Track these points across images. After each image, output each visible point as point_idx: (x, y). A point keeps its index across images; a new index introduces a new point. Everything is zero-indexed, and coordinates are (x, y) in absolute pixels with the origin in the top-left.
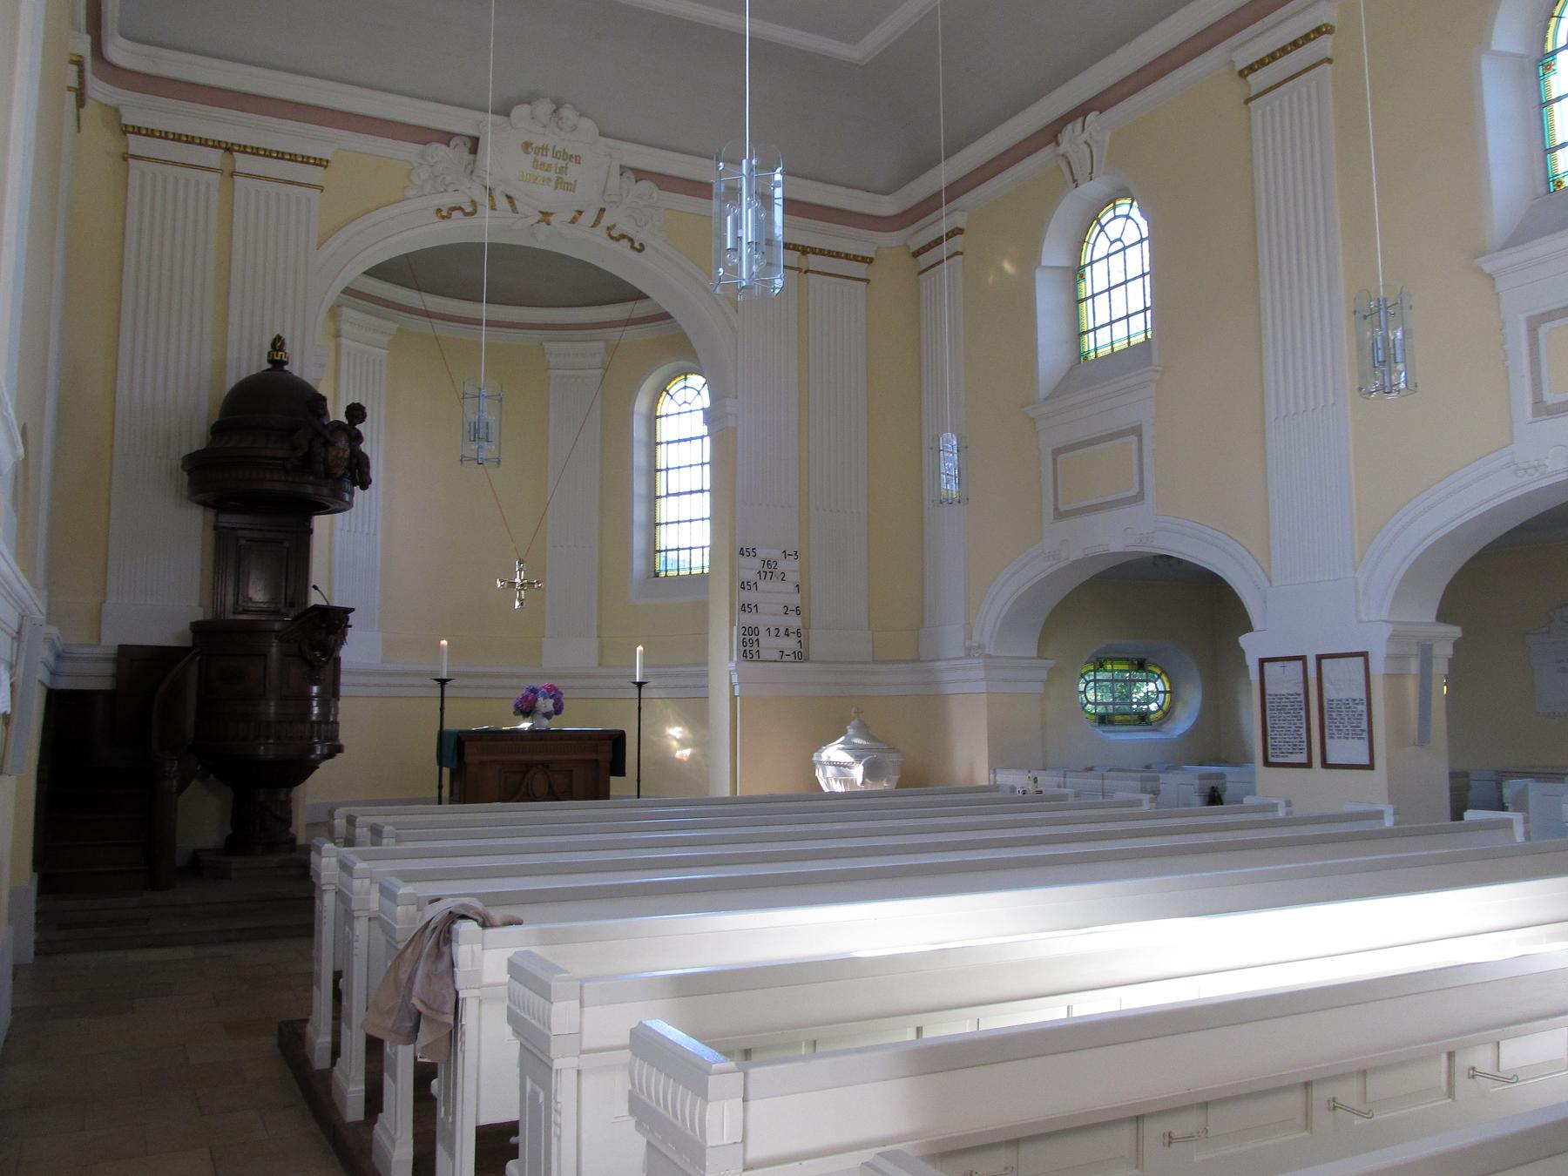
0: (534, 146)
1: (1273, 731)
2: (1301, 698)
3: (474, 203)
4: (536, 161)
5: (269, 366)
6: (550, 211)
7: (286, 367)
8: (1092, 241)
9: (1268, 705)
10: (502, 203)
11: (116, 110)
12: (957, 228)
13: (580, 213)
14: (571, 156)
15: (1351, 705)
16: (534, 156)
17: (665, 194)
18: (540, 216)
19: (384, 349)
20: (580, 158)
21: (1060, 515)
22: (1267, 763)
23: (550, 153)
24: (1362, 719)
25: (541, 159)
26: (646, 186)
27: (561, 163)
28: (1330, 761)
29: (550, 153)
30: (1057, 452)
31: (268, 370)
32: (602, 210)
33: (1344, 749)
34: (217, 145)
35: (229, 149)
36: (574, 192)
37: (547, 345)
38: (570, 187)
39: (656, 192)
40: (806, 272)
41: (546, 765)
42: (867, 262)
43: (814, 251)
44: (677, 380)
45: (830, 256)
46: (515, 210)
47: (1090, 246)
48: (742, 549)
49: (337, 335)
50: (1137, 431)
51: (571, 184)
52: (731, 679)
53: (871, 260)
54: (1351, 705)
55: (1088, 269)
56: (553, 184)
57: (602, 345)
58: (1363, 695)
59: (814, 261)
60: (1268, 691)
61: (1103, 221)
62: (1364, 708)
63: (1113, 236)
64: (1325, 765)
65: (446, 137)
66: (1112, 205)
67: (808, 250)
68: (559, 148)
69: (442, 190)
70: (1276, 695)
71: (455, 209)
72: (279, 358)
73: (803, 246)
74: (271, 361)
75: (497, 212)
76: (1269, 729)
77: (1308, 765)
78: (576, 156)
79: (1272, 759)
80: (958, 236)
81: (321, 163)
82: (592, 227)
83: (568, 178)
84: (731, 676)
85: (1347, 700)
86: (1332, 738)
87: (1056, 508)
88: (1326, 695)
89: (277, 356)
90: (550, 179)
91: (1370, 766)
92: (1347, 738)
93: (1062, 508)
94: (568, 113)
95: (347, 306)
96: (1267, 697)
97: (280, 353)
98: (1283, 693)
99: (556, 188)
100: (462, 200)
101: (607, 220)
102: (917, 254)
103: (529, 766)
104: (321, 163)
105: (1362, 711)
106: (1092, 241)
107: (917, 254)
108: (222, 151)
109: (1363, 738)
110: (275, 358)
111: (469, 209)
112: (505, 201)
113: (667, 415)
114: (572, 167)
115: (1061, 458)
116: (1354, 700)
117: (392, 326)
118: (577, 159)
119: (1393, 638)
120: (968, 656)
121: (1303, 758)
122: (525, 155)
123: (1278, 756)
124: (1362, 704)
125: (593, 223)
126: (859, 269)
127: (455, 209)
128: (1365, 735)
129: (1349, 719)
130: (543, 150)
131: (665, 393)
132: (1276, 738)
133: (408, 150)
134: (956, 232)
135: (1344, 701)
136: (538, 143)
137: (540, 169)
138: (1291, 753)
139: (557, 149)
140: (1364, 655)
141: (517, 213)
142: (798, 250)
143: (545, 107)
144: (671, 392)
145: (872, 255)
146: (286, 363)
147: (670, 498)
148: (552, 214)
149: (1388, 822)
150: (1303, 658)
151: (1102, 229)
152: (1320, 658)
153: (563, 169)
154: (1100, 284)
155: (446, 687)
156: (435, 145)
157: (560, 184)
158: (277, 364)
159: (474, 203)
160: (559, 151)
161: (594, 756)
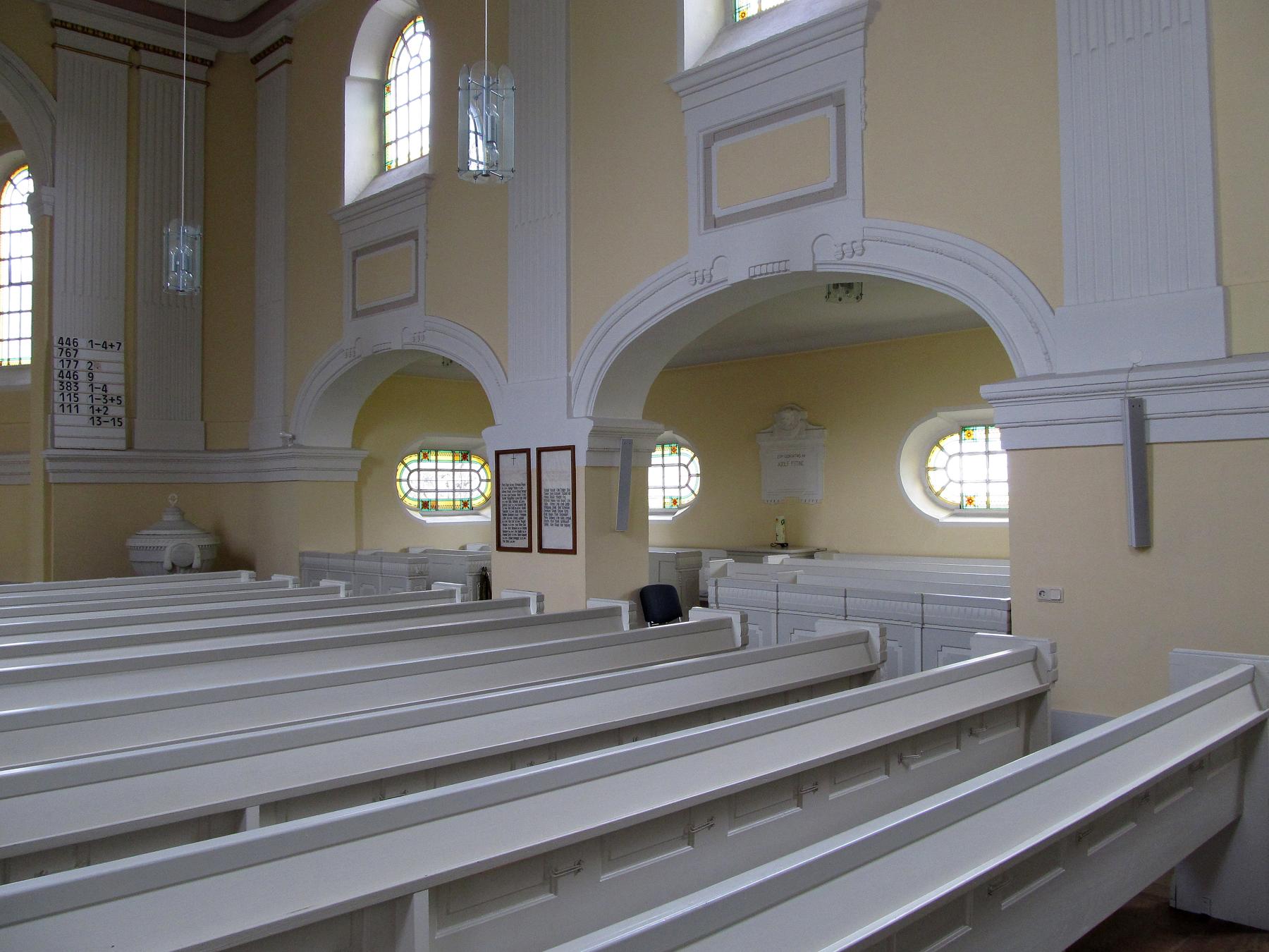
1: (505, 518)
2: (525, 488)
8: (396, 56)
9: (501, 493)
12: (286, 37)
21: (357, 314)
28: (545, 546)
30: (357, 254)
33: (557, 536)
40: (138, 68)
42: (207, 65)
43: (147, 47)
44: (21, 170)
45: (165, 54)
47: (395, 60)
48: (62, 338)
50: (413, 236)
52: (45, 466)
53: (211, 62)
55: (393, 82)
59: (146, 57)
60: (502, 482)
61: (406, 37)
62: (569, 497)
63: (413, 52)
64: (541, 550)
66: (413, 22)
67: (142, 46)
70: (508, 485)
73: (135, 41)
76: (502, 516)
77: (529, 550)
79: (503, 544)
80: (287, 45)
84: (44, 463)
86: (547, 525)
87: (354, 308)
88: (544, 487)
91: (573, 551)
93: (359, 308)
96: (501, 486)
98: (512, 483)
102: (256, 60)
106: (396, 56)
107: (256, 60)
109: (569, 525)
113: (10, 205)
115: (359, 260)
116: (563, 490)
119: (595, 433)
120: (284, 447)
121: (525, 544)
123: (508, 541)
129: (560, 508)
131: (9, 183)
134: (287, 40)
135: (556, 491)
138: (517, 539)
140: (572, 448)
144: (14, 182)
145: (212, 58)
147: (12, 287)
149: (533, 611)
150: (527, 451)
151: (405, 43)
152: (540, 451)
154: (402, 100)
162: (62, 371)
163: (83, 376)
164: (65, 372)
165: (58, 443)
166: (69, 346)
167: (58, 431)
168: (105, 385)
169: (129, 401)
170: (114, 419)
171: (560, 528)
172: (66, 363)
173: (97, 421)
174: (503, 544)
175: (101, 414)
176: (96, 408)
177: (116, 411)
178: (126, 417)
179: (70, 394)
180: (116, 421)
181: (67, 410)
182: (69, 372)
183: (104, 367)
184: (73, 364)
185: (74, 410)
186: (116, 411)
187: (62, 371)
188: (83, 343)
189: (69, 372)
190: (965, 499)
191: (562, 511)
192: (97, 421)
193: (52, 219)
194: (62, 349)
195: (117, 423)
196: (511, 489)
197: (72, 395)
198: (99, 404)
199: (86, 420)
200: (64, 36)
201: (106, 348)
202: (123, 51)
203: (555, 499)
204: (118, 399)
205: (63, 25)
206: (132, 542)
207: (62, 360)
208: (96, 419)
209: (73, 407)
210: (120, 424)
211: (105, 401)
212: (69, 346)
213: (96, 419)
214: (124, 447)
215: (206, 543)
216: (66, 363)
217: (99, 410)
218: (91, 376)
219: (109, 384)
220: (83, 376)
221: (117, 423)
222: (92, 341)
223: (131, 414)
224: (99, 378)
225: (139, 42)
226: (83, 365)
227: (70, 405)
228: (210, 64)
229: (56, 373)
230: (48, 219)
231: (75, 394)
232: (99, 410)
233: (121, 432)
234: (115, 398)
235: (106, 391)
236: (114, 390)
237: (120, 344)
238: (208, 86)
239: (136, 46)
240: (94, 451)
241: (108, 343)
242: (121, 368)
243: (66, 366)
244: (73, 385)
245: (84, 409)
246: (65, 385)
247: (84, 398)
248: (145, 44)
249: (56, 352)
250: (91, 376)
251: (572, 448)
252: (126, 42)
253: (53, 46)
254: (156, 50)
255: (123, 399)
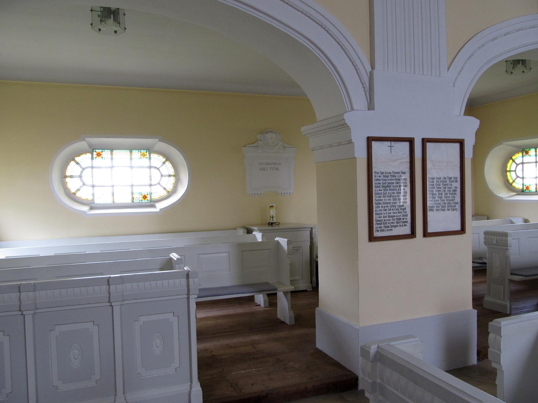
1: (378, 207)
15: (448, 182)
22: (372, 238)
24: (456, 194)
54: (448, 182)
58: (458, 175)
60: (374, 170)
62: (458, 185)
70: (382, 173)
79: (376, 234)
85: (445, 178)
86: (432, 210)
92: (444, 210)
98: (389, 171)
105: (456, 187)
109: (456, 209)
116: (450, 178)
121: (407, 230)
123: (383, 231)
124: (456, 181)
128: (458, 207)
132: (380, 214)
135: (442, 179)
138: (395, 226)
152: (425, 141)
171: (446, 212)
174: (376, 234)
190: (525, 187)
191: (449, 197)
196: (387, 177)
203: (441, 186)
251: (461, 143)
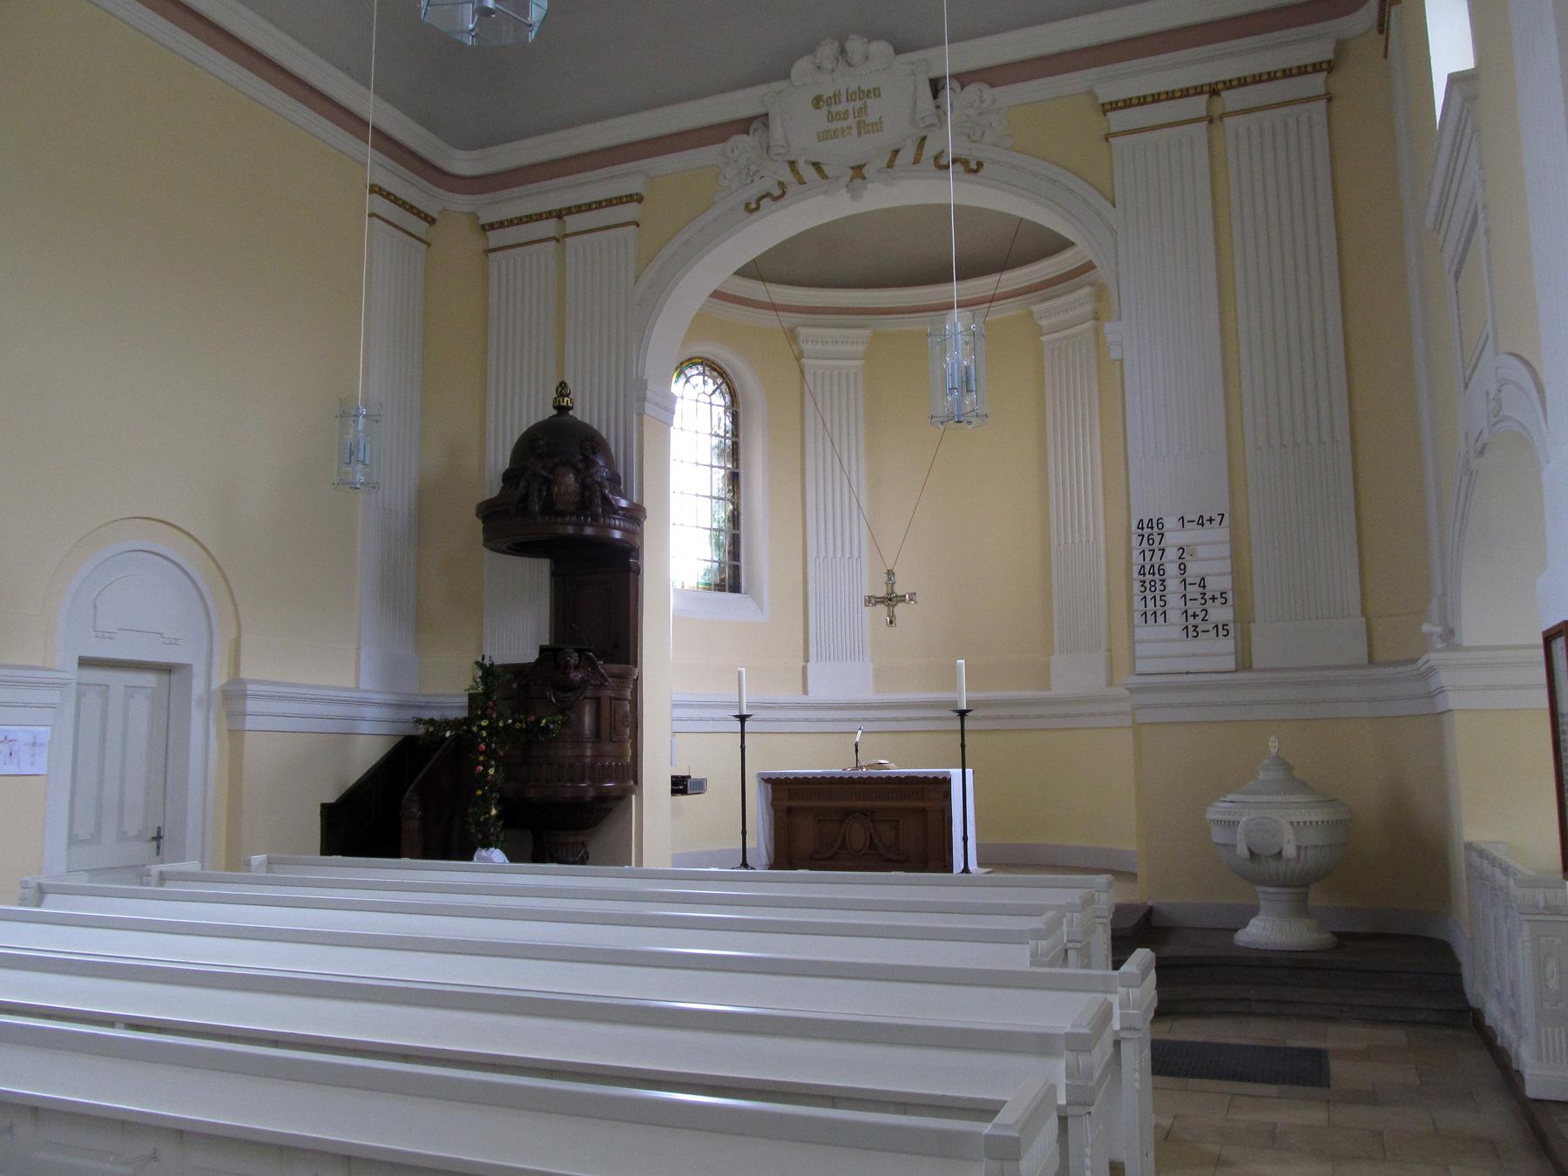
0: (824, 98)
3: (781, 185)
4: (829, 112)
5: (555, 412)
6: (862, 163)
7: (571, 413)
10: (808, 173)
11: (475, 214)
13: (896, 152)
14: (869, 91)
16: (827, 108)
17: (997, 90)
18: (851, 172)
19: (858, 359)
20: (879, 89)
23: (844, 98)
25: (835, 109)
26: (973, 89)
27: (858, 104)
29: (844, 98)
31: (554, 416)
32: (924, 138)
34: (549, 215)
35: (559, 214)
36: (882, 131)
37: (1034, 308)
38: (877, 127)
39: (988, 93)
40: (1221, 118)
41: (868, 814)
43: (1229, 85)
46: (824, 176)
49: (799, 357)
51: (877, 123)
53: (1329, 62)
56: (855, 130)
57: (1086, 290)
59: (1231, 99)
65: (743, 126)
68: (853, 87)
69: (749, 181)
71: (763, 197)
72: (565, 404)
73: (1210, 85)
74: (554, 407)
75: (807, 185)
78: (874, 90)
81: (636, 198)
82: (914, 163)
83: (872, 117)
89: (563, 401)
90: (850, 128)
94: (855, 46)
95: (805, 325)
97: (566, 399)
99: (860, 134)
100: (770, 185)
101: (930, 150)
103: (848, 813)
104: (636, 198)
108: (555, 220)
110: (562, 404)
111: (777, 192)
112: (812, 170)
114: (871, 102)
117: (866, 333)
118: (876, 92)
122: (818, 111)
125: (913, 161)
126: (1316, 83)
127: (763, 197)
130: (836, 97)
133: (710, 154)
136: (827, 93)
137: (837, 120)
139: (850, 91)
141: (805, 183)
142: (1201, 93)
143: (827, 51)
145: (1330, 56)
146: (571, 408)
148: (864, 165)
153: (862, 111)
155: (747, 724)
156: (736, 137)
157: (863, 128)
158: (562, 410)
159: (781, 185)
160: (854, 92)
161: (921, 804)
162: (1143, 567)
163: (1172, 569)
164: (1147, 568)
165: (1142, 666)
166: (1151, 530)
167: (1140, 649)
168: (1203, 579)
169: (1240, 595)
170: (1217, 626)
172: (1148, 554)
173: (1192, 632)
175: (1198, 620)
176: (1190, 613)
177: (1220, 614)
178: (1234, 622)
179: (1155, 597)
180: (1221, 629)
181: (1151, 619)
182: (1153, 566)
183: (1202, 551)
184: (1158, 554)
185: (1160, 619)
186: (1220, 614)
187: (1143, 567)
188: (1170, 522)
189: (1153, 566)
192: (1192, 632)
193: (1121, 361)
194: (1143, 536)
195: (1221, 632)
197: (1158, 598)
198: (1194, 607)
199: (1176, 632)
200: (1118, 120)
201: (1203, 524)
202: (1198, 105)
204: (1222, 597)
205: (1115, 106)
206: (1213, 813)
207: (1144, 551)
208: (1191, 629)
209: (1156, 615)
210: (1225, 633)
211: (1203, 601)
212: (1151, 530)
213: (1191, 629)
214: (1230, 663)
215: (1315, 818)
216: (1148, 554)
217: (1195, 616)
218: (1183, 568)
219: (1209, 575)
220: (1172, 569)
221: (1221, 632)
222: (1182, 518)
223: (1244, 618)
224: (1194, 570)
225: (1217, 83)
226: (1172, 554)
227: (1155, 613)
228: (1329, 67)
229: (1136, 569)
230: (1118, 363)
231: (1161, 596)
232: (1195, 616)
233: (1227, 645)
234: (1218, 595)
235: (1204, 587)
236: (1214, 586)
237: (1223, 515)
238: (1329, 100)
239: (1214, 91)
240: (1190, 676)
241: (1206, 517)
242: (1225, 550)
243: (1148, 558)
244: (1158, 583)
245: (1175, 616)
246: (1147, 585)
247: (1174, 600)
248: (1224, 82)
249: (1135, 540)
250: (1183, 568)
252: (1198, 91)
253: (1106, 138)
254: (1242, 82)
255: (1229, 596)
